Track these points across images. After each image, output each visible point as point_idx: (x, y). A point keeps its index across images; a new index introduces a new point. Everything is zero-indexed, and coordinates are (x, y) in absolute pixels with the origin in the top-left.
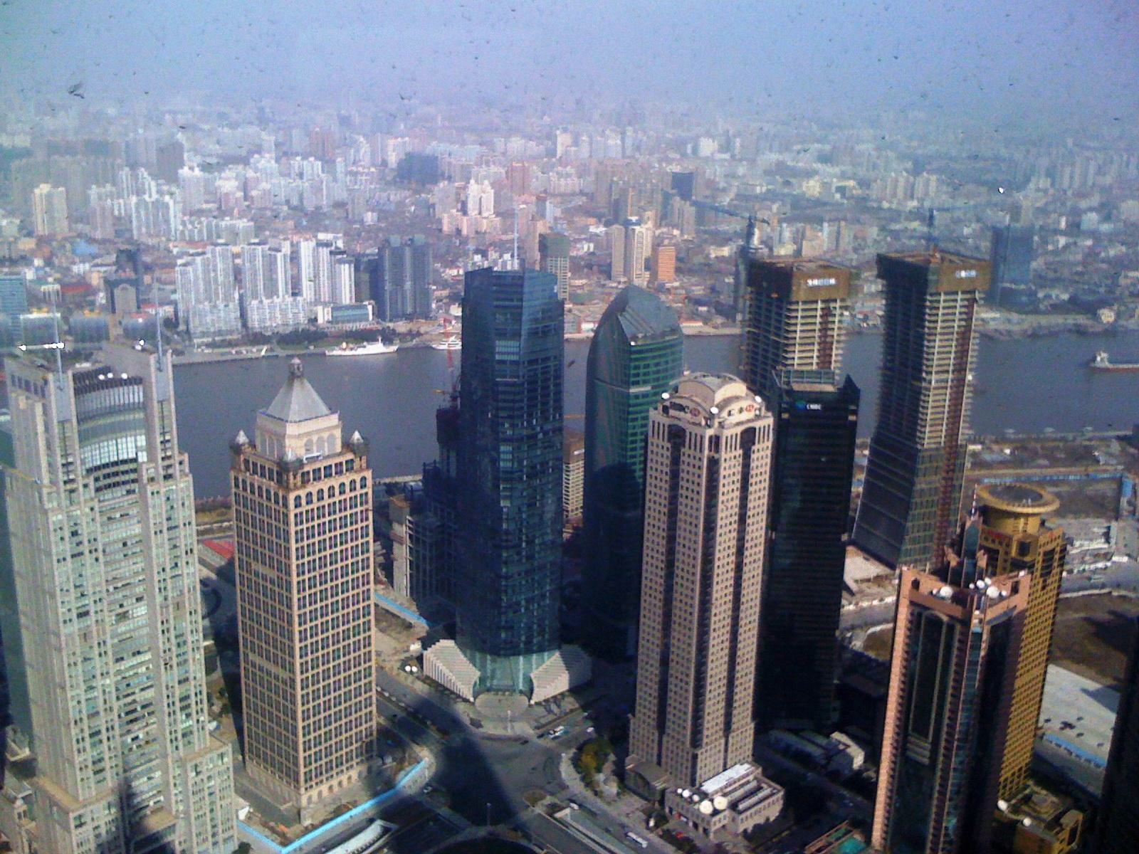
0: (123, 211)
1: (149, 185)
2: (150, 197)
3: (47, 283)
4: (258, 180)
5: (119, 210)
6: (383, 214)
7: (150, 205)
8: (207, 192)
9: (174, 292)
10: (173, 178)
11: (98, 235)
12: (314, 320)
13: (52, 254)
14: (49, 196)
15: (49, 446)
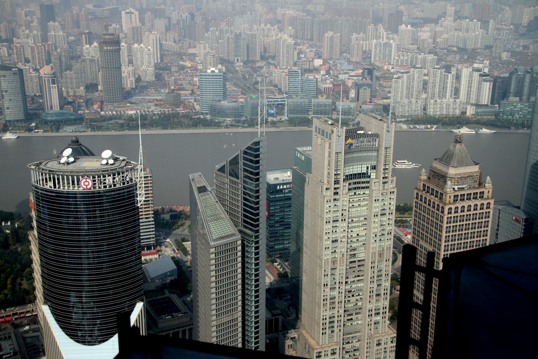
0: (367, 49)
1: (383, 34)
2: (383, 41)
3: (326, 83)
4: (442, 33)
5: (366, 47)
6: (514, 54)
7: (382, 44)
8: (413, 39)
9: (390, 92)
10: (396, 31)
11: (354, 59)
12: (464, 113)
13: (330, 68)
14: (332, 38)
15: (329, 165)
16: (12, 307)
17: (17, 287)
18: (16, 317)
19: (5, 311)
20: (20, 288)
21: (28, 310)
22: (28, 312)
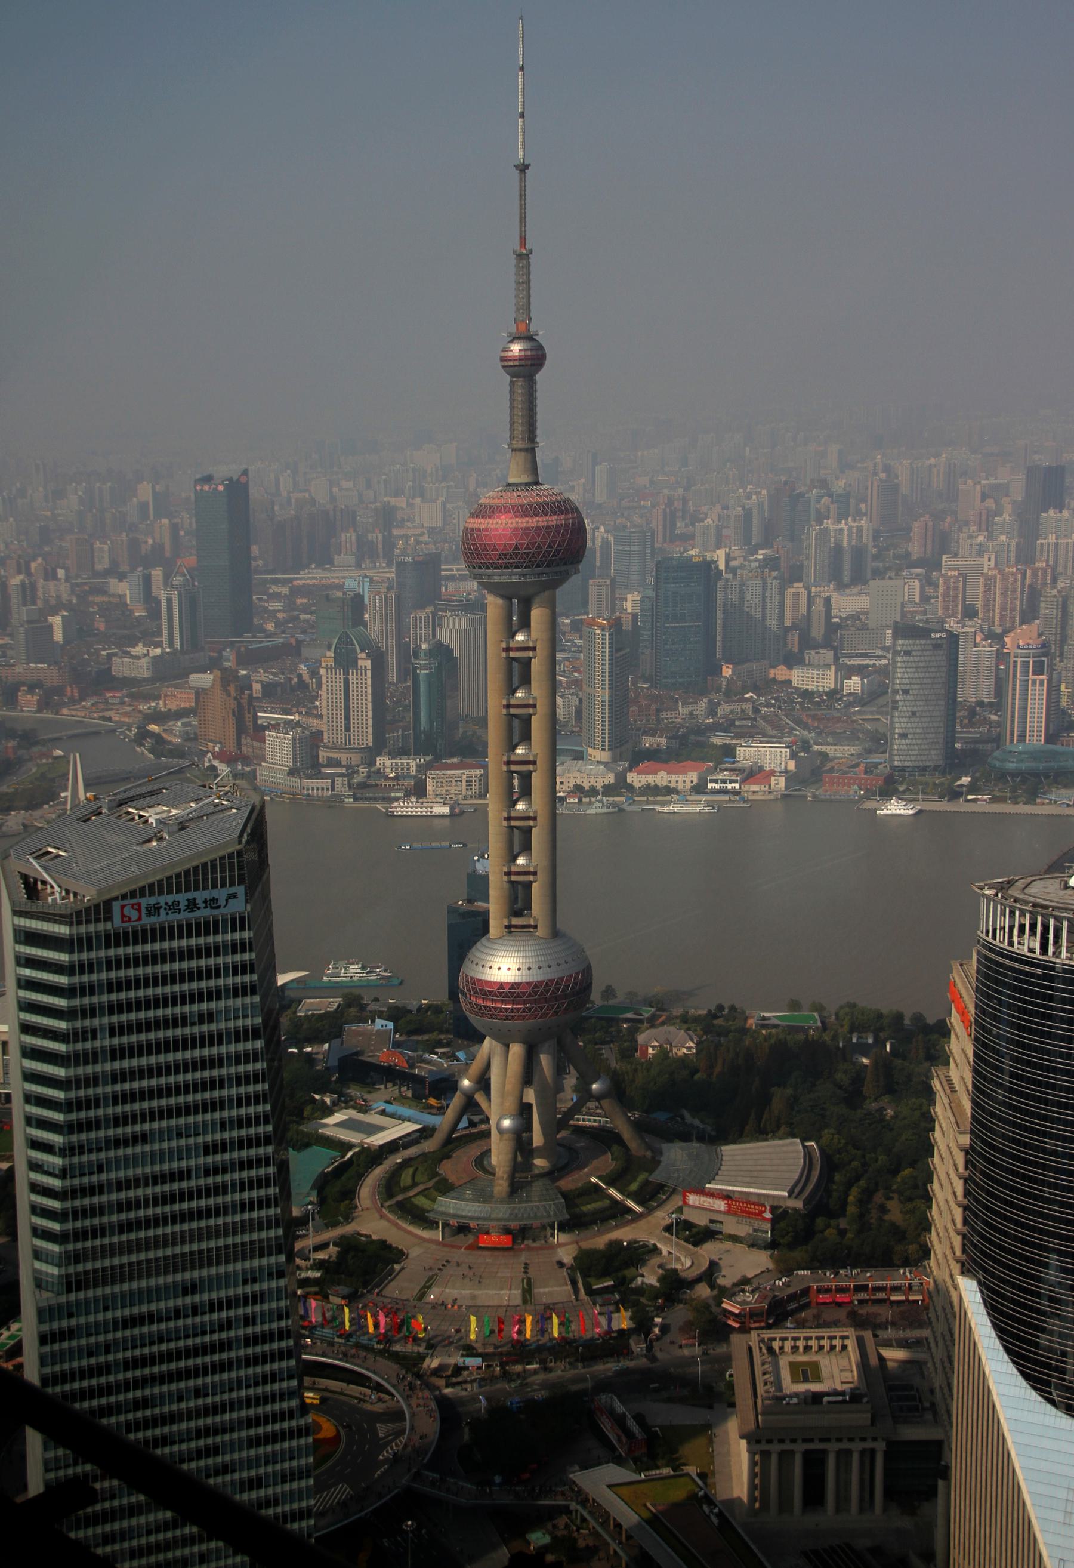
16: (853, 1267)
17: (874, 1213)
18: (863, 1296)
19: (837, 1274)
20: (881, 1219)
21: (897, 1283)
22: (896, 1289)
